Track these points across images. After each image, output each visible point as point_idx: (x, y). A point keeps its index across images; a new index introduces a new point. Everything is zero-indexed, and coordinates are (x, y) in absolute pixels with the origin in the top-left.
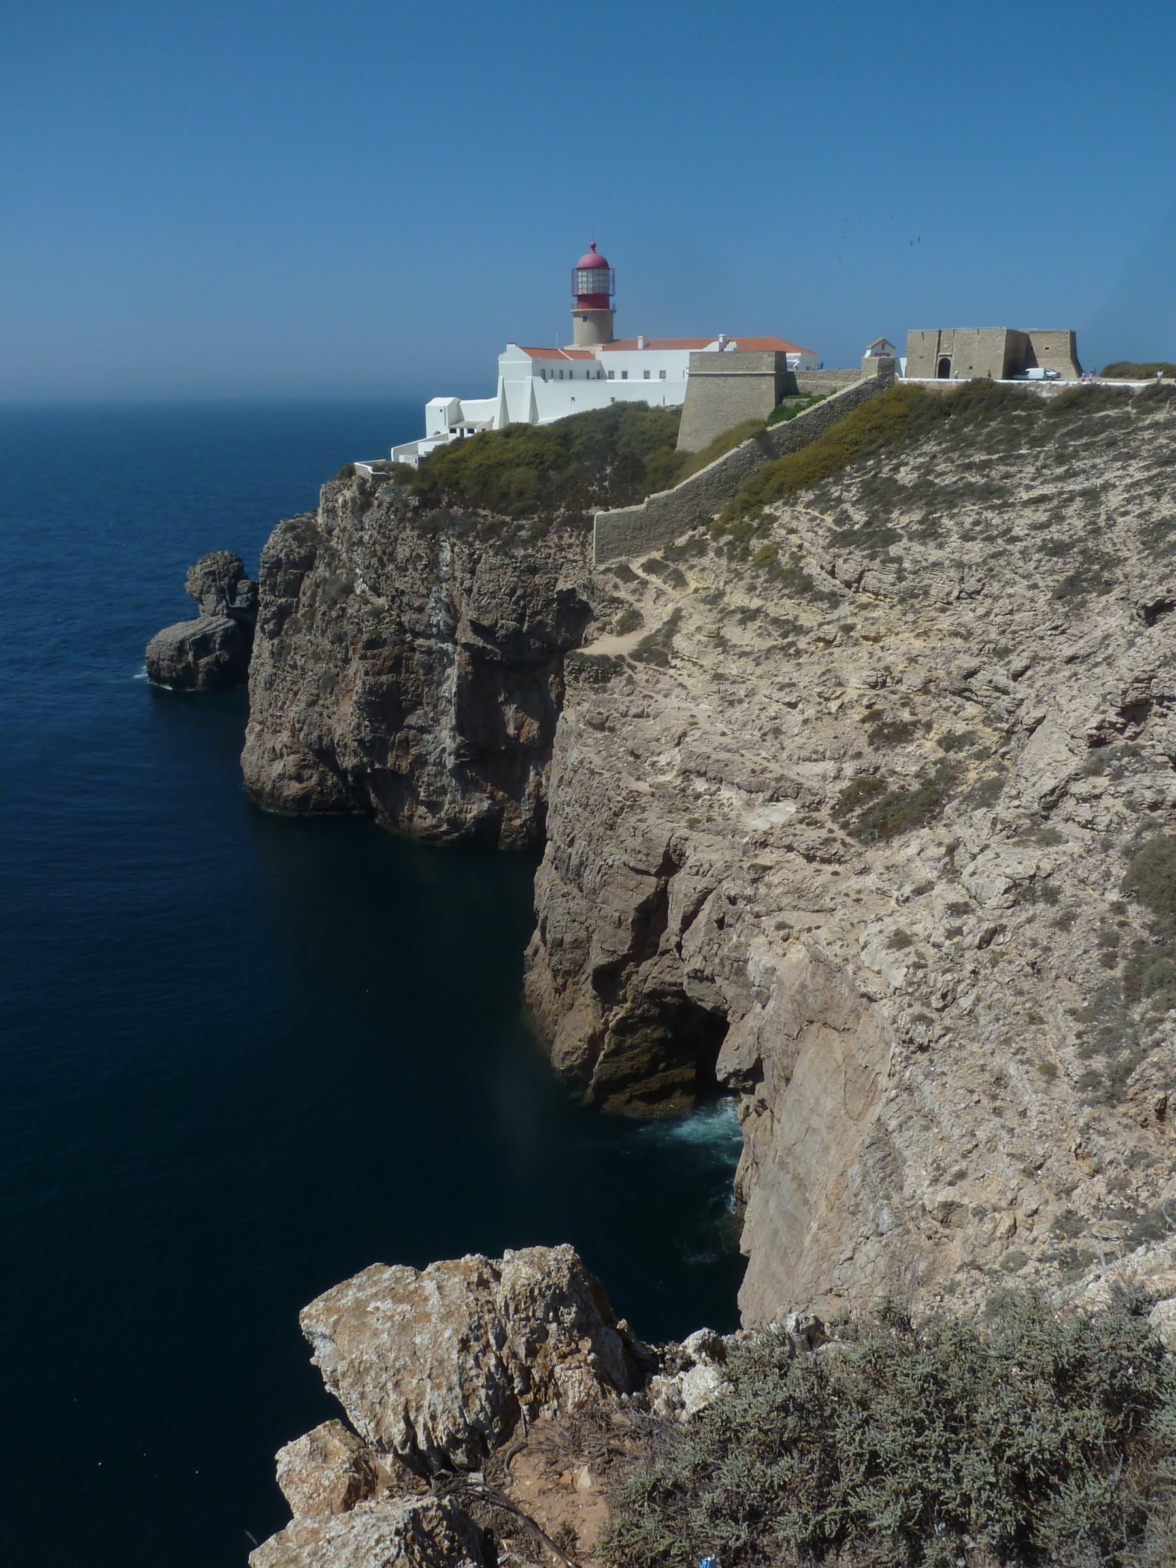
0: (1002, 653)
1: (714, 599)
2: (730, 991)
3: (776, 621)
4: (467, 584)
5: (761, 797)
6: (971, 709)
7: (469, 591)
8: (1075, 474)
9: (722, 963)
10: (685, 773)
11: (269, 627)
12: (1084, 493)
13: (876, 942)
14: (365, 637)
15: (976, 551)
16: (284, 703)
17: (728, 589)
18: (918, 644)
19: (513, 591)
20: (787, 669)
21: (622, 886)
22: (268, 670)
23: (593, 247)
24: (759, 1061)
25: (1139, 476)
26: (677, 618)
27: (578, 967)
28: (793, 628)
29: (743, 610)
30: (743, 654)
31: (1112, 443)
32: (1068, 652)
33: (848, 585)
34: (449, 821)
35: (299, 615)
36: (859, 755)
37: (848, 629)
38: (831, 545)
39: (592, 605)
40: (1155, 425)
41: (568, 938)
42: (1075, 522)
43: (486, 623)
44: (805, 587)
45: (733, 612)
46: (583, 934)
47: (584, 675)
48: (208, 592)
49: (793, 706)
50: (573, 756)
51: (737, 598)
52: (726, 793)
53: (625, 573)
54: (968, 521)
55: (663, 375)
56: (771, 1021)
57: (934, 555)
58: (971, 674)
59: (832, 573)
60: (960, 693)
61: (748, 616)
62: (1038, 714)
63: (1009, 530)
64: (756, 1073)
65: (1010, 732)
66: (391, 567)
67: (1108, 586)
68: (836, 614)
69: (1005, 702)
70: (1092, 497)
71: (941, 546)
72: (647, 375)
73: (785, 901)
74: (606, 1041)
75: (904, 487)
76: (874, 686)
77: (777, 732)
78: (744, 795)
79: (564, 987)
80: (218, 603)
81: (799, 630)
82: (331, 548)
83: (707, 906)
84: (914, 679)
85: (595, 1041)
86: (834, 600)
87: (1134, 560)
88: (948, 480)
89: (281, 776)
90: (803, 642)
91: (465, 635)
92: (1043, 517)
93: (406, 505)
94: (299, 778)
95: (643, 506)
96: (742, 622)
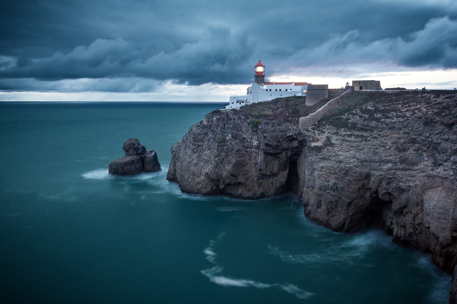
0: (421, 135)
1: (337, 134)
2: (395, 194)
3: (358, 136)
4: (266, 135)
5: (383, 163)
6: (416, 145)
7: (265, 137)
8: (411, 106)
9: (393, 189)
10: (362, 162)
11: (195, 150)
12: (416, 109)
13: (442, 171)
14: (236, 149)
15: (401, 119)
16: (201, 169)
17: (338, 131)
18: (398, 136)
19: (277, 136)
20: (370, 143)
21: (353, 184)
22: (196, 161)
23: (260, 61)
24: (407, 203)
25: (425, 106)
26: (328, 139)
27: (336, 206)
28: (362, 136)
29: (348, 135)
30: (355, 142)
31: (414, 101)
32: (437, 132)
33: (373, 128)
34: (253, 194)
35: (204, 147)
36: (398, 154)
37: (379, 135)
38: (364, 121)
39: (298, 138)
40: (420, 97)
41: (333, 200)
42: (419, 114)
43: (270, 144)
44: (360, 129)
45: (344, 135)
46: (337, 198)
47: (314, 150)
48: (131, 149)
49: (377, 148)
50: (321, 165)
51: (344, 133)
52: (372, 164)
53: (307, 130)
54: (395, 115)
55: (280, 90)
56: (412, 194)
57: (393, 121)
58: (416, 138)
59: (368, 126)
60: (413, 142)
61: (350, 136)
62: (440, 141)
63: (406, 116)
64: (406, 206)
65: (429, 148)
66: (241, 132)
67: (436, 123)
68: (373, 133)
69: (425, 143)
70: (419, 110)
71: (393, 119)
72: (276, 90)
73: (403, 176)
74: (348, 219)
75: (371, 111)
76: (394, 143)
77: (377, 153)
78: (378, 163)
79: (331, 212)
80: (133, 152)
81: (365, 137)
82: (212, 130)
83: (384, 181)
84: (402, 141)
85: (345, 220)
86: (372, 131)
87: (438, 119)
88: (382, 108)
89: (200, 188)
90: (369, 139)
91: (262, 146)
92: (411, 113)
93: (242, 118)
94: (206, 188)
95: (309, 116)
96: (348, 137)
